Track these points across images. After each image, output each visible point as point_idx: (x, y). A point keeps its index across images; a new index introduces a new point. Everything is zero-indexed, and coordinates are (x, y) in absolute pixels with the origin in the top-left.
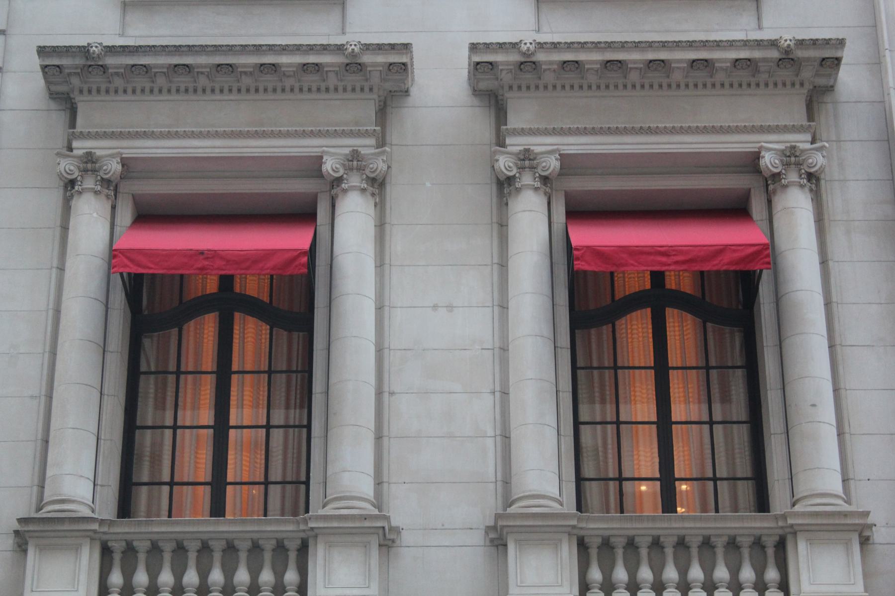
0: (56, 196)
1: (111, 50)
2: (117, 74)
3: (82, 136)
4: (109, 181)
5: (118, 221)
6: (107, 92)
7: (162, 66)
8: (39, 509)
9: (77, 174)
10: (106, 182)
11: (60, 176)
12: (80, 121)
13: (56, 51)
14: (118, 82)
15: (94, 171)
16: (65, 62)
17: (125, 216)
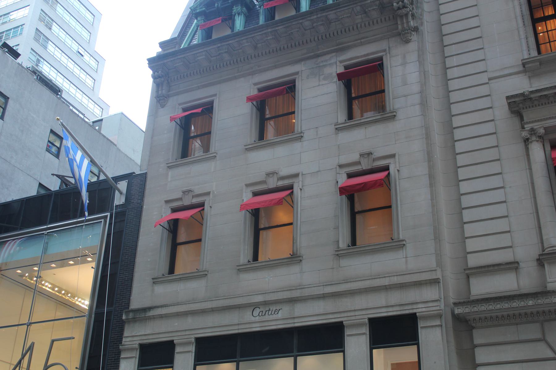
0: (522, 146)
1: (532, 92)
2: (536, 100)
3: (527, 123)
4: (540, 136)
5: (546, 149)
6: (533, 106)
7: (552, 94)
8: (543, 251)
9: (529, 136)
10: (540, 137)
11: (523, 138)
12: (525, 118)
13: (512, 97)
14: (536, 103)
15: (535, 134)
16: (517, 99)
17: (548, 148)
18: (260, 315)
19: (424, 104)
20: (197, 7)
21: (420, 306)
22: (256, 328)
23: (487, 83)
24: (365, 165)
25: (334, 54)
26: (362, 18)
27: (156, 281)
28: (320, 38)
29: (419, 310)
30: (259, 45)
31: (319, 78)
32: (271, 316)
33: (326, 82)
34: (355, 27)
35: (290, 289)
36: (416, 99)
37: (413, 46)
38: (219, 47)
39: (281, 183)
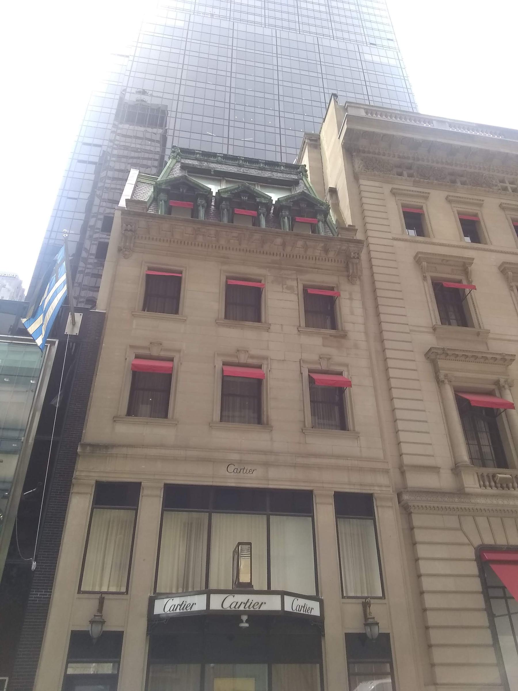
18: (235, 471)
19: (366, 333)
20: (162, 183)
21: (376, 488)
22: (231, 483)
23: (409, 333)
24: (324, 366)
25: (295, 272)
26: (320, 253)
27: (116, 419)
28: (285, 255)
29: (375, 490)
30: (232, 241)
31: (283, 287)
32: (245, 475)
33: (289, 291)
34: (314, 258)
35: (265, 453)
36: (361, 328)
37: (357, 288)
38: (199, 228)
39: (250, 361)
